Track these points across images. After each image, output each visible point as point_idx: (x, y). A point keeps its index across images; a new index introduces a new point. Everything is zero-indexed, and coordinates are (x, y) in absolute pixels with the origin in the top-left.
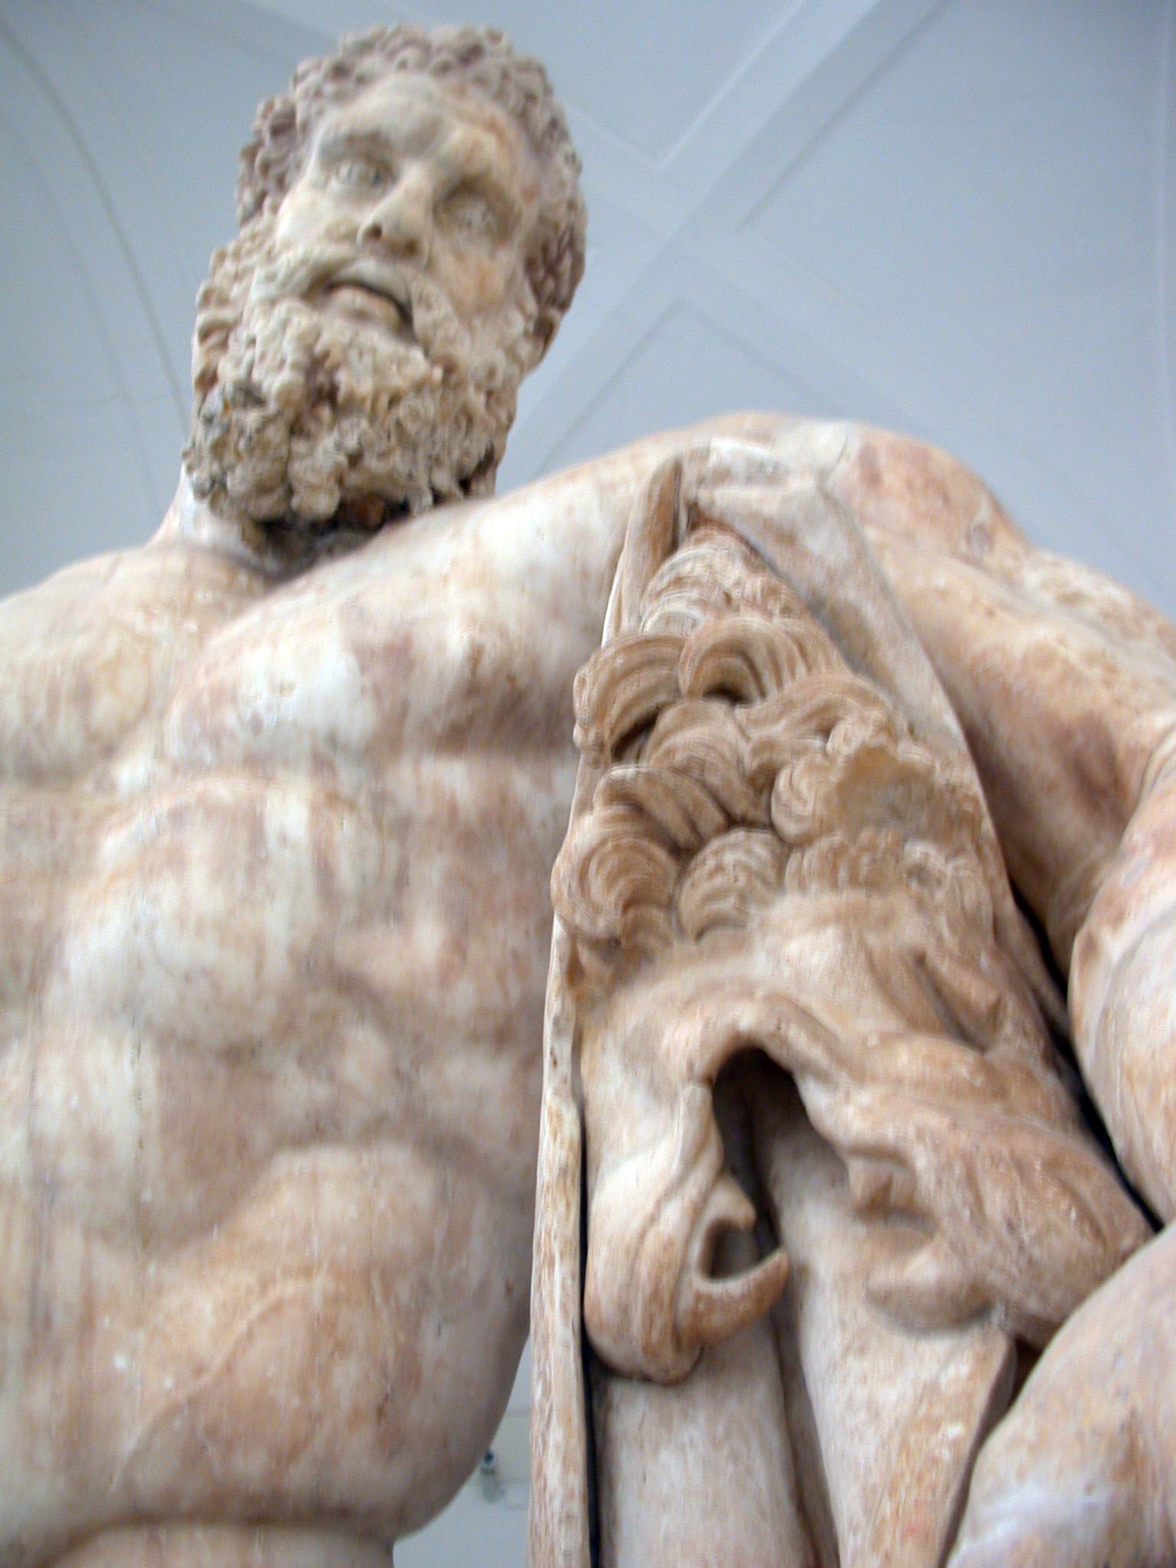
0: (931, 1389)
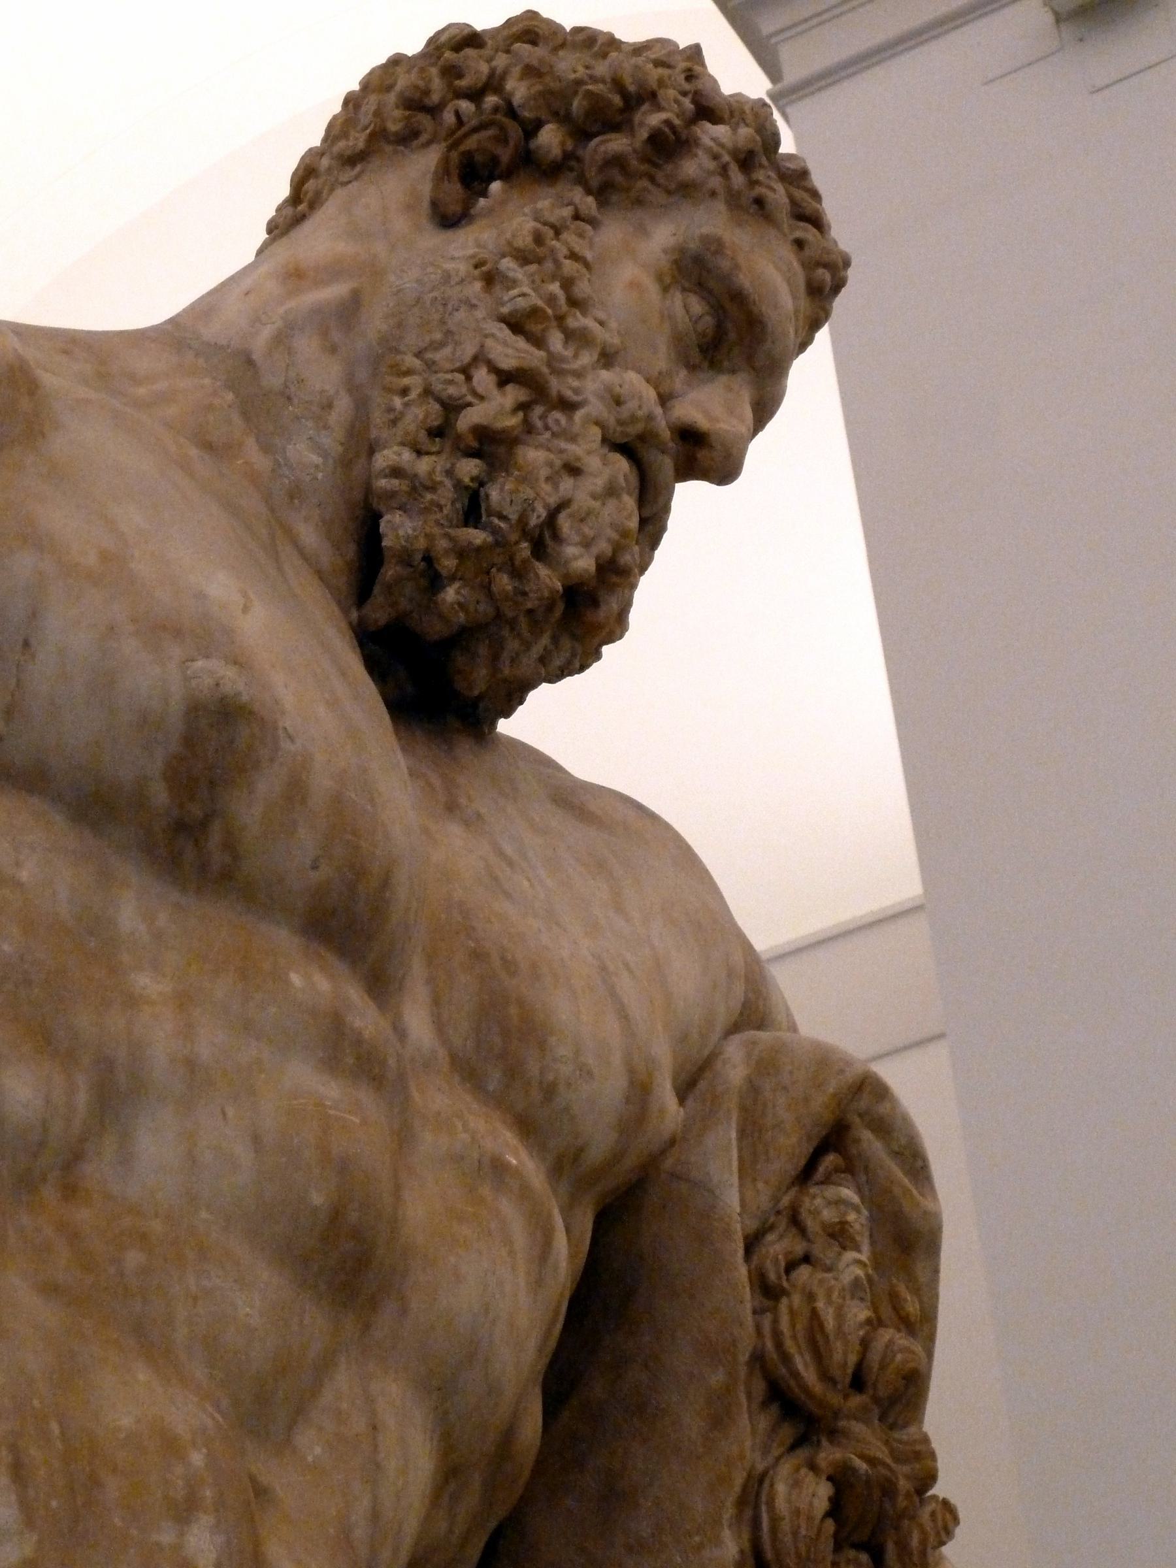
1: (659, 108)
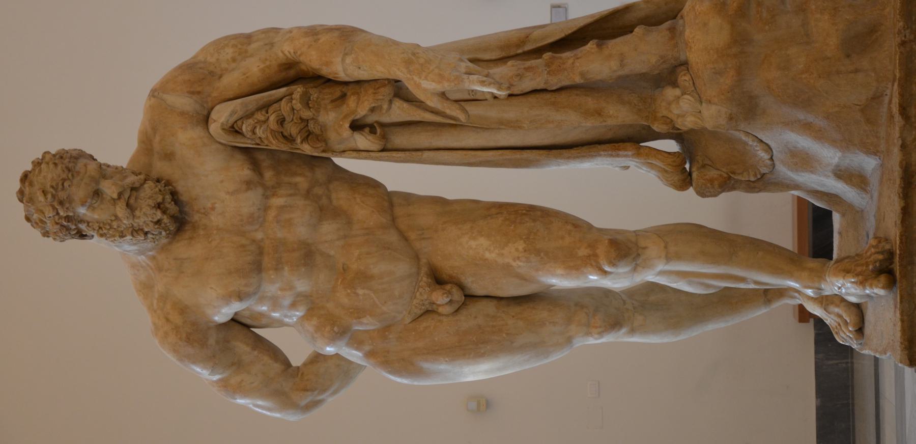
0: (399, 107)
1: (62, 223)
